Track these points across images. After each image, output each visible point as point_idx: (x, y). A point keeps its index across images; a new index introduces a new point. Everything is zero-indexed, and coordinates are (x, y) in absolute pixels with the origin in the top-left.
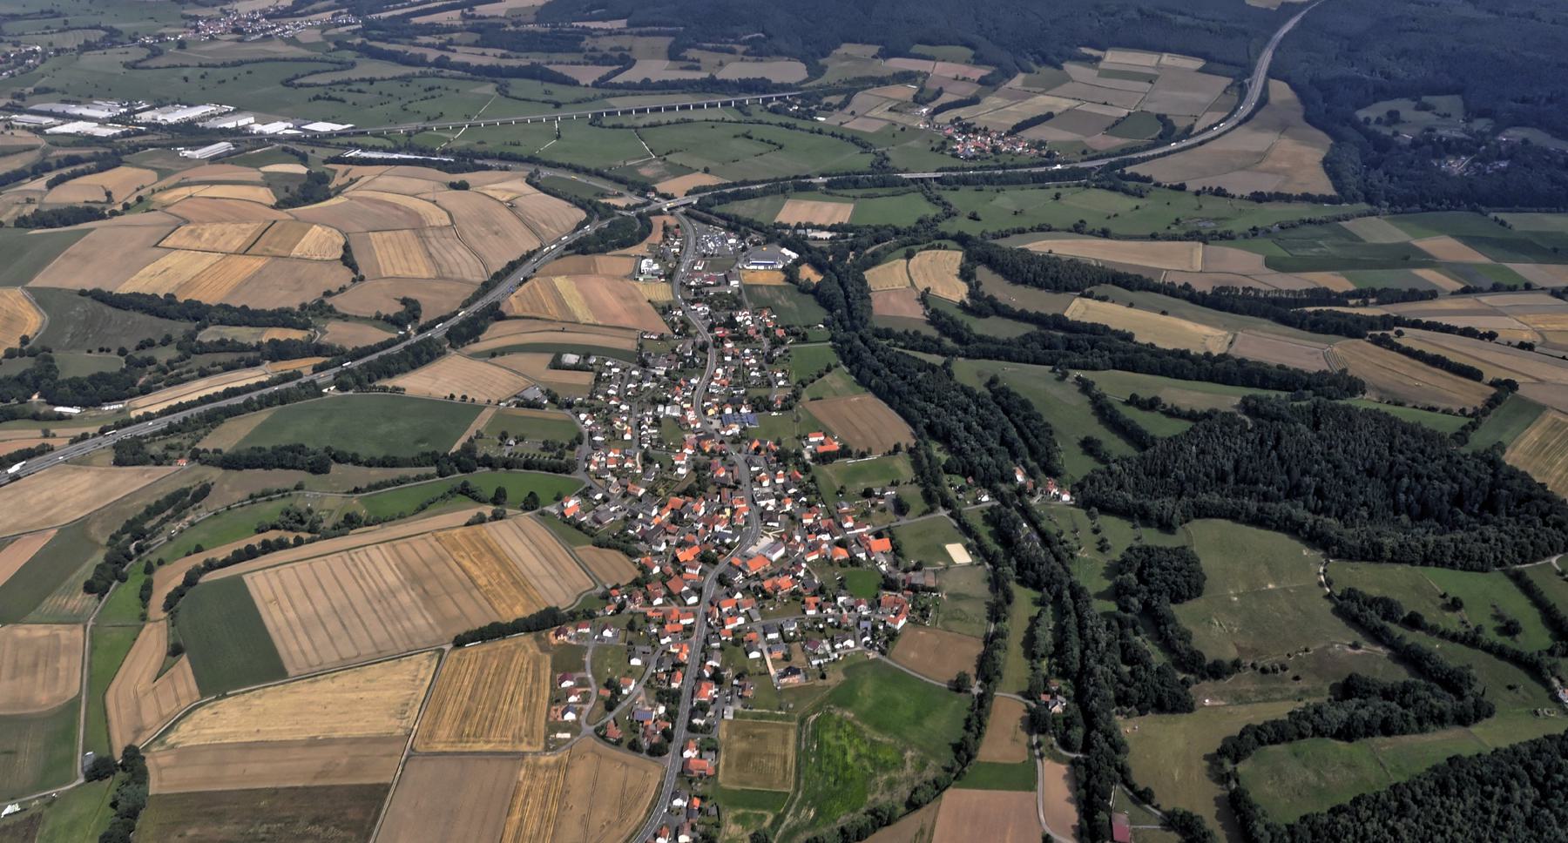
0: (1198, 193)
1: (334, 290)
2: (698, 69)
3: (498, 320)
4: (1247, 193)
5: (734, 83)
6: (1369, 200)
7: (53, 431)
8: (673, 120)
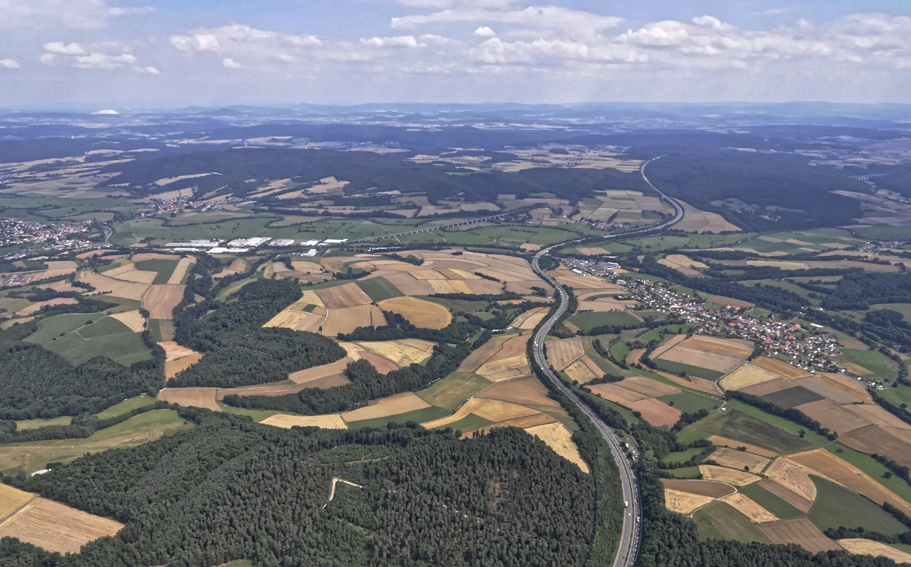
0: (703, 233)
6: (755, 231)
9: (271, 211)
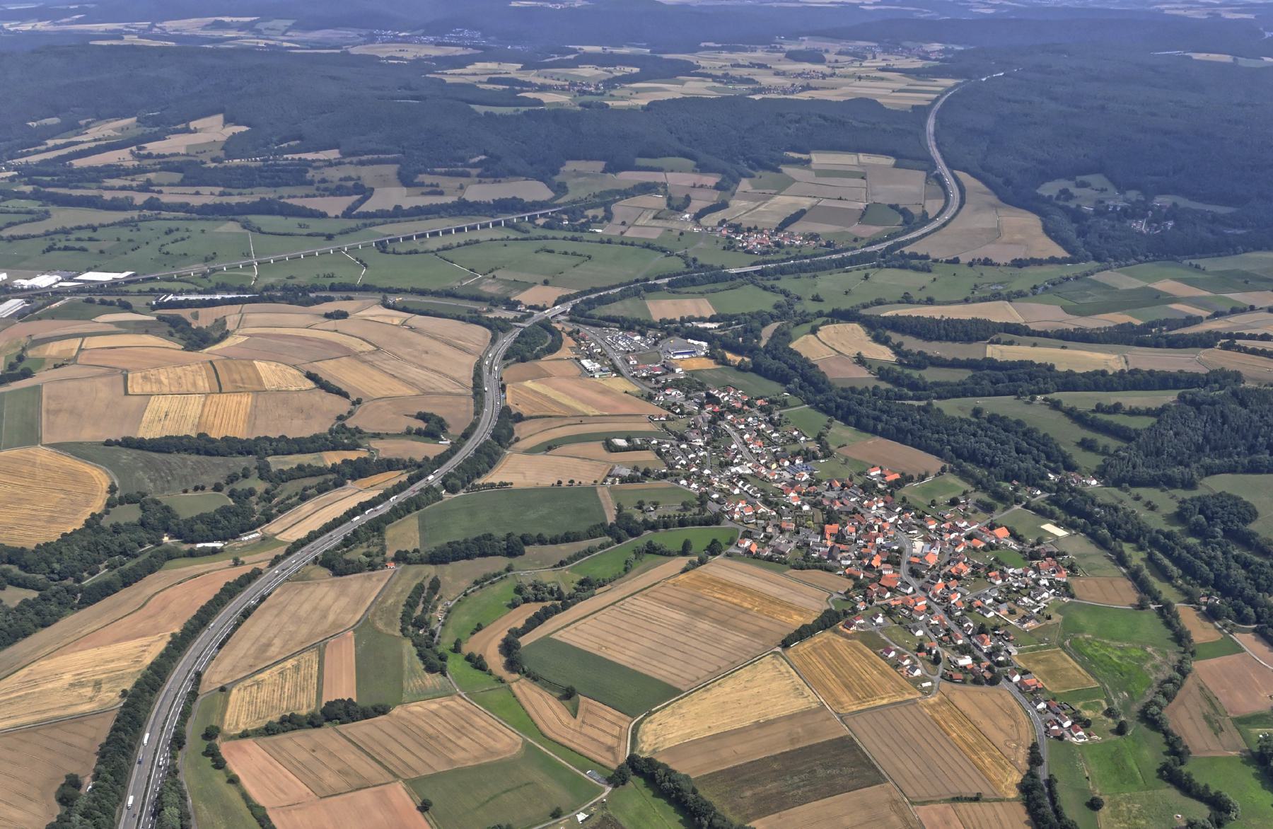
0: (971, 265)
1: (345, 414)
2: (441, 193)
3: (517, 422)
5: (488, 204)
6: (1097, 258)
8: (462, 242)
9: (35, 196)
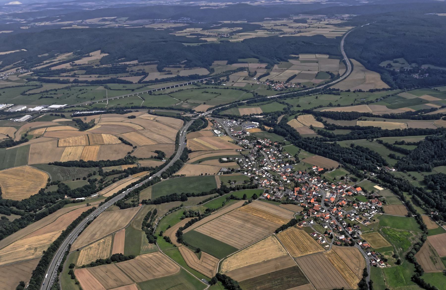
0: (354, 92)
1: (131, 152)
2: (171, 74)
3: (190, 153)
4: (368, 90)
5: (187, 77)
6: (400, 88)
7: (90, 204)
8: (177, 90)
9: (39, 80)
